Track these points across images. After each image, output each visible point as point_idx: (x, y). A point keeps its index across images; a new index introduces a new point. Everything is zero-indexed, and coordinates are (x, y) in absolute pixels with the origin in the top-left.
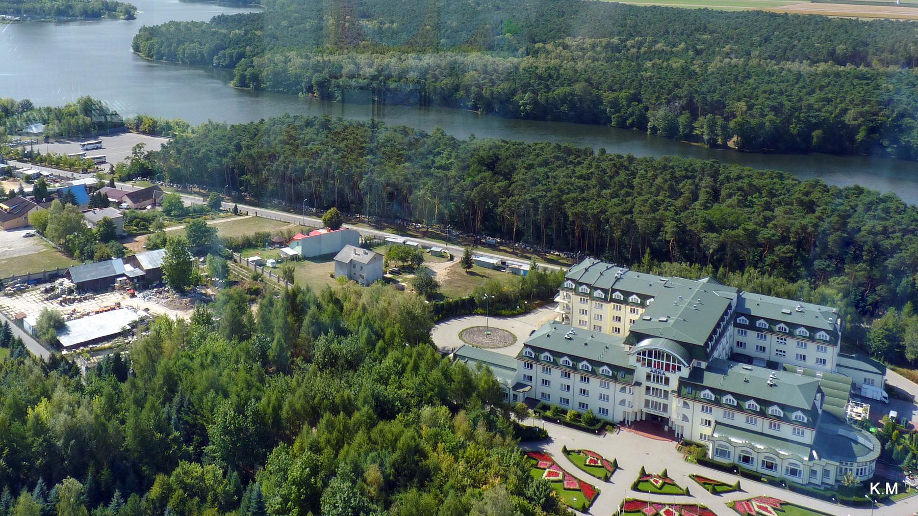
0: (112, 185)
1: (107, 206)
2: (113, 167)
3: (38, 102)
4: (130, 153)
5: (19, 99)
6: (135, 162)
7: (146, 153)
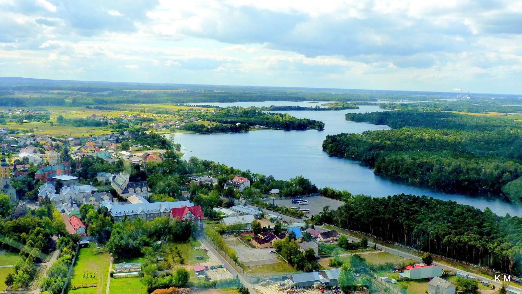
0: (313, 227)
1: (310, 240)
3: (277, 178)
4: (322, 212)
5: (267, 175)
6: (324, 216)
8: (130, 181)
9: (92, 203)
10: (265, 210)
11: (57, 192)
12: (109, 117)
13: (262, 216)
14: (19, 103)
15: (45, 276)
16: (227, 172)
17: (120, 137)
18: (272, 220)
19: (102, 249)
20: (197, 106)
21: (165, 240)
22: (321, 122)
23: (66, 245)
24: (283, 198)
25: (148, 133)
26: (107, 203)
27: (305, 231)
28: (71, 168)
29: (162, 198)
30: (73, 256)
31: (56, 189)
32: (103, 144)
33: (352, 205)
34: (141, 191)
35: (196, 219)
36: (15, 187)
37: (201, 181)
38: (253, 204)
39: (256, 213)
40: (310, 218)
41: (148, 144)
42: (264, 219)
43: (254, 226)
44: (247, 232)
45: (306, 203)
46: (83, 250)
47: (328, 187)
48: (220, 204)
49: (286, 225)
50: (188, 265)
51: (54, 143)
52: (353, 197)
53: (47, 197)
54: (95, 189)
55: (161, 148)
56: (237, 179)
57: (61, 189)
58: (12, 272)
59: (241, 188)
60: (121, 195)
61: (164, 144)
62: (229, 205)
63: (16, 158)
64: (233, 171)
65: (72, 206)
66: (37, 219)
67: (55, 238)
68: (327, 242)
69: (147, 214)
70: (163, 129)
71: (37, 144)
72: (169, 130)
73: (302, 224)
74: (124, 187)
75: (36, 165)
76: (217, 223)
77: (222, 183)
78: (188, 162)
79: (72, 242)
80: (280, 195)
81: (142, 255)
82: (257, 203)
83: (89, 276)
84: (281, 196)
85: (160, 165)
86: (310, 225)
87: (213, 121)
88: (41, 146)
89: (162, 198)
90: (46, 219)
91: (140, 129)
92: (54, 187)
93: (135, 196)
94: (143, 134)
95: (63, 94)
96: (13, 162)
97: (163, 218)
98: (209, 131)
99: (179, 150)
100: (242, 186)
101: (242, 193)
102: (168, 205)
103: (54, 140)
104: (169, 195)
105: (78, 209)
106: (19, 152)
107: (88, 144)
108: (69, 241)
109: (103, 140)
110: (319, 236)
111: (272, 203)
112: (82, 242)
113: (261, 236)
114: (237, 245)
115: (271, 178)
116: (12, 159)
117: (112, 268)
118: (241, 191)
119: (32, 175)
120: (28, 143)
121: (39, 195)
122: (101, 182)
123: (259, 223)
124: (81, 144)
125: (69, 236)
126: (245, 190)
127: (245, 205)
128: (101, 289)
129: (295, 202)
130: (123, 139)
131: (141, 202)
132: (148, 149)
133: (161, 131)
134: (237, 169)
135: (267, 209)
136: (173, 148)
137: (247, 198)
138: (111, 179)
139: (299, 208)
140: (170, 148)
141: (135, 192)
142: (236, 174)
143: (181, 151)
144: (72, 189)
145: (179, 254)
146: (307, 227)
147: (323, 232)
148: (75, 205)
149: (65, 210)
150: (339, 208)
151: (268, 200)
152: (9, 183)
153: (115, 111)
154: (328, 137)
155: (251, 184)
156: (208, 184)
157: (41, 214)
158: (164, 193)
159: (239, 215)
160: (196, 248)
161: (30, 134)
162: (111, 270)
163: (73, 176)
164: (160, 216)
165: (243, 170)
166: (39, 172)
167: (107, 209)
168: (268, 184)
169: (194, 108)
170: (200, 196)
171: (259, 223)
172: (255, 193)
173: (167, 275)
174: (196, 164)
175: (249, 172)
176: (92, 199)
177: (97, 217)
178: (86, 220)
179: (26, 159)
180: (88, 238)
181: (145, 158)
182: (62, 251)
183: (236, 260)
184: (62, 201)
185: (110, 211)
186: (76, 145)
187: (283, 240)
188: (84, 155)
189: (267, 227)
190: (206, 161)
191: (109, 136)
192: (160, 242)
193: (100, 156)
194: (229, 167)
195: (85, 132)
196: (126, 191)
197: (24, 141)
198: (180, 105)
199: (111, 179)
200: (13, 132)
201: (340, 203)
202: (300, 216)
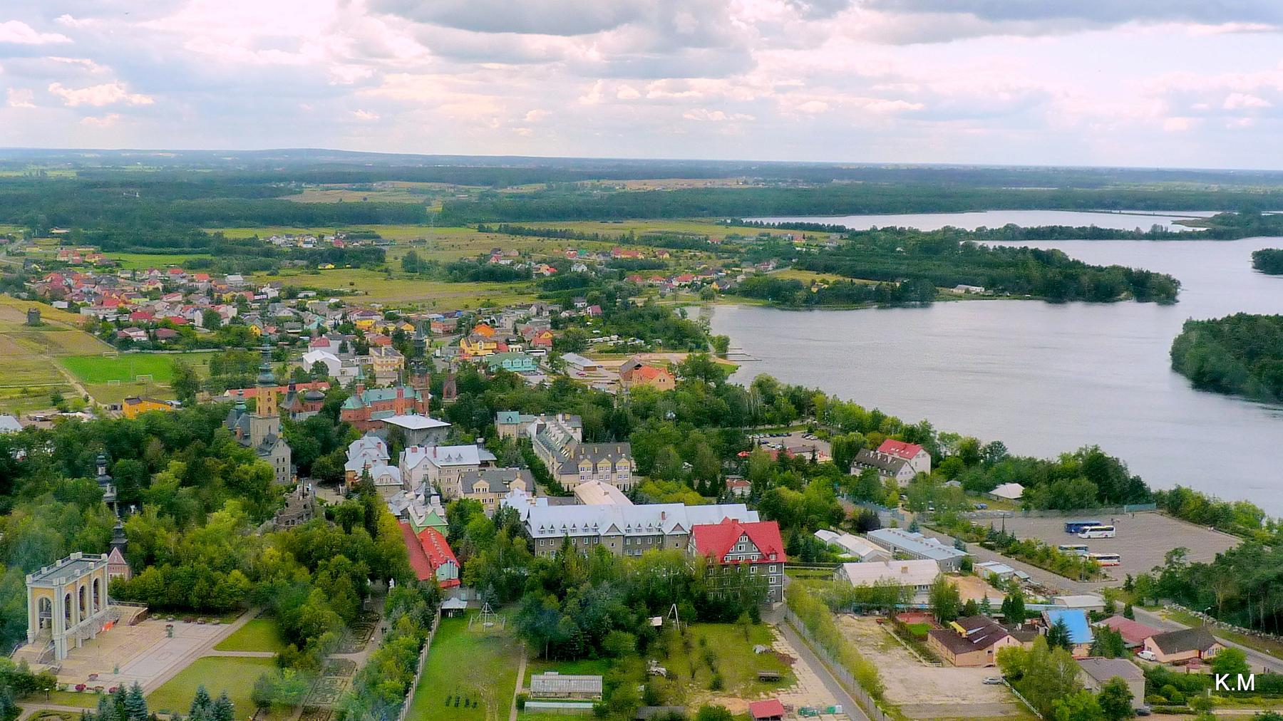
0: (1128, 614)
2: (1130, 579)
3: (1017, 450)
4: (1162, 563)
5: (985, 441)
6: (1169, 576)
7: (1189, 565)
8: (584, 440)
9: (480, 497)
10: (974, 549)
11: (393, 461)
13: (965, 567)
14: (310, 217)
16: (860, 427)
17: (564, 314)
18: (994, 581)
21: (673, 617)
22: (1168, 278)
24: (1034, 512)
25: (640, 302)
26: (520, 498)
27: (1102, 625)
28: (430, 396)
31: (390, 449)
32: (516, 331)
33: (1267, 549)
34: (614, 470)
35: (764, 562)
36: (289, 443)
37: (784, 449)
38: (938, 528)
39: (945, 557)
40: (1122, 581)
42: (971, 577)
43: (938, 595)
44: (917, 612)
45: (1109, 534)
47: (1184, 486)
48: (835, 519)
49: (1040, 598)
50: (734, 696)
51: (392, 327)
52: (1271, 526)
53: (365, 472)
55: (674, 348)
56: (891, 451)
57: (402, 454)
59: (903, 478)
60: (557, 478)
61: (682, 336)
62: (863, 526)
63: (297, 365)
64: (876, 423)
65: (427, 501)
66: (337, 531)
68: (1176, 664)
69: (625, 538)
71: (346, 328)
72: (698, 296)
73: (1096, 601)
74: (567, 454)
75: (344, 384)
76: (825, 578)
77: (846, 455)
78: (747, 388)
80: (1026, 502)
82: (952, 523)
84: (1027, 508)
85: (670, 396)
86: (1120, 604)
92: (384, 447)
93: (594, 482)
94: (626, 306)
97: (670, 549)
99: (724, 357)
100: (905, 468)
101: (904, 492)
102: (685, 515)
103: (391, 318)
104: (690, 485)
105: (441, 511)
106: (305, 346)
107: (480, 331)
109: (518, 321)
110: (1149, 642)
111: (998, 529)
112: (447, 606)
113: (960, 629)
114: (884, 649)
115: (997, 448)
116: (288, 368)
117: (527, 684)
118: (900, 485)
119: (333, 410)
120: (328, 324)
121: (348, 467)
122: (506, 438)
123: (954, 587)
124: (458, 331)
126: (914, 481)
127: (913, 529)
129: (1073, 529)
130: (571, 320)
132: (635, 350)
133: (675, 298)
134: (890, 416)
135: (982, 545)
136: (706, 349)
137: (921, 509)
138: (532, 430)
139: (1086, 549)
140: (698, 346)
141: (595, 470)
142: (889, 432)
143: (730, 358)
144: (430, 455)
145: (709, 660)
146: (1110, 610)
147: (1161, 630)
148: (435, 499)
149: (410, 510)
150: (1219, 557)
151: (986, 516)
152: (275, 431)
154: (1190, 326)
155: (934, 466)
156: (801, 460)
157: (349, 519)
158: (677, 480)
159: (898, 557)
160: (760, 648)
161: (333, 300)
162: (519, 690)
163: (434, 417)
164: (661, 547)
165: (910, 419)
166: (350, 404)
167: (516, 513)
168: (989, 464)
170: (777, 493)
171: (954, 587)
172: (947, 493)
174: (770, 400)
175: (926, 428)
176: (482, 484)
178: (461, 543)
179: (320, 368)
180: (464, 596)
183: (877, 696)
184: (402, 487)
185: (526, 523)
186: (447, 333)
187: (1029, 646)
188: (465, 362)
189: (978, 601)
190: (799, 388)
191: (534, 310)
192: (657, 621)
193: (507, 365)
194: (869, 410)
196: (571, 467)
197: (318, 319)
199: (532, 430)
200: (292, 294)
201: (1227, 542)
202: (1089, 572)
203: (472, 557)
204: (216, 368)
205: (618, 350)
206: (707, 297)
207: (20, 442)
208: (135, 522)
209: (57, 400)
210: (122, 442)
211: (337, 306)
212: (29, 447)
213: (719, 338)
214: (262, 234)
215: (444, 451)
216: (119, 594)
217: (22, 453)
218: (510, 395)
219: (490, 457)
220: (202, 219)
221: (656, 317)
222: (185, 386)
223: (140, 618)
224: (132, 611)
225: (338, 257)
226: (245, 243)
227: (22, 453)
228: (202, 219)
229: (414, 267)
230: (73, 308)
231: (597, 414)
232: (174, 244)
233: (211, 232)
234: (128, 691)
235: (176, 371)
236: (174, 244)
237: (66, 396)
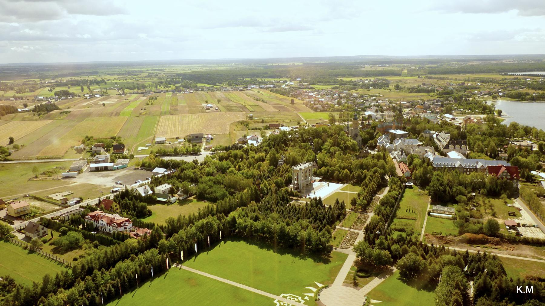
12: (437, 85)
14: (368, 74)
15: (378, 203)
17: (445, 102)
19: (422, 191)
20: (522, 75)
23: (395, 184)
29: (479, 156)
30: (399, 193)
34: (461, 148)
41: (470, 109)
46: (407, 190)
54: (421, 143)
55: (482, 113)
58: (356, 197)
61: (485, 109)
65: (402, 154)
67: (387, 177)
69: (464, 168)
70: (486, 96)
72: (491, 97)
74: (445, 144)
79: (399, 182)
81: (456, 202)
83: (411, 211)
87: (540, 89)
88: (381, 107)
89: (479, 156)
90: (382, 161)
91: (463, 95)
94: (466, 100)
95: (401, 67)
96: (361, 118)
98: (533, 99)
104: (487, 154)
106: (366, 111)
108: (398, 181)
112: (407, 184)
117: (430, 208)
120: (373, 104)
125: (398, 177)
128: (419, 223)
130: (447, 104)
131: (459, 157)
132: (469, 113)
133: (483, 98)
136: (494, 113)
138: (435, 136)
141: (455, 148)
148: (404, 154)
149: (396, 156)
153: (442, 81)
157: (379, 157)
162: (428, 209)
163: (404, 131)
167: (429, 159)
169: (519, 77)
173: (478, 223)
177: (421, 166)
178: (411, 167)
179: (370, 117)
181: (466, 121)
182: (391, 188)
191: (435, 101)
195: (415, 97)
198: (505, 75)
199: (435, 136)
203: (415, 171)
204: (340, 116)
205: (462, 114)
206: (495, 98)
207: (290, 133)
208: (319, 155)
209: (299, 123)
210: (317, 134)
211: (375, 99)
212: (292, 135)
213: (499, 111)
214: (354, 79)
215: (408, 141)
216: (315, 174)
217: (290, 136)
218: (428, 126)
219: (421, 143)
220: (337, 76)
221: (476, 104)
222: (332, 120)
223: (320, 181)
224: (319, 179)
225: (375, 85)
226: (348, 82)
227: (290, 136)
228: (337, 76)
229: (398, 88)
230: (302, 99)
231: (456, 132)
232: (329, 82)
233: (339, 79)
234: (318, 198)
235: (330, 116)
236: (329, 82)
237: (301, 122)
